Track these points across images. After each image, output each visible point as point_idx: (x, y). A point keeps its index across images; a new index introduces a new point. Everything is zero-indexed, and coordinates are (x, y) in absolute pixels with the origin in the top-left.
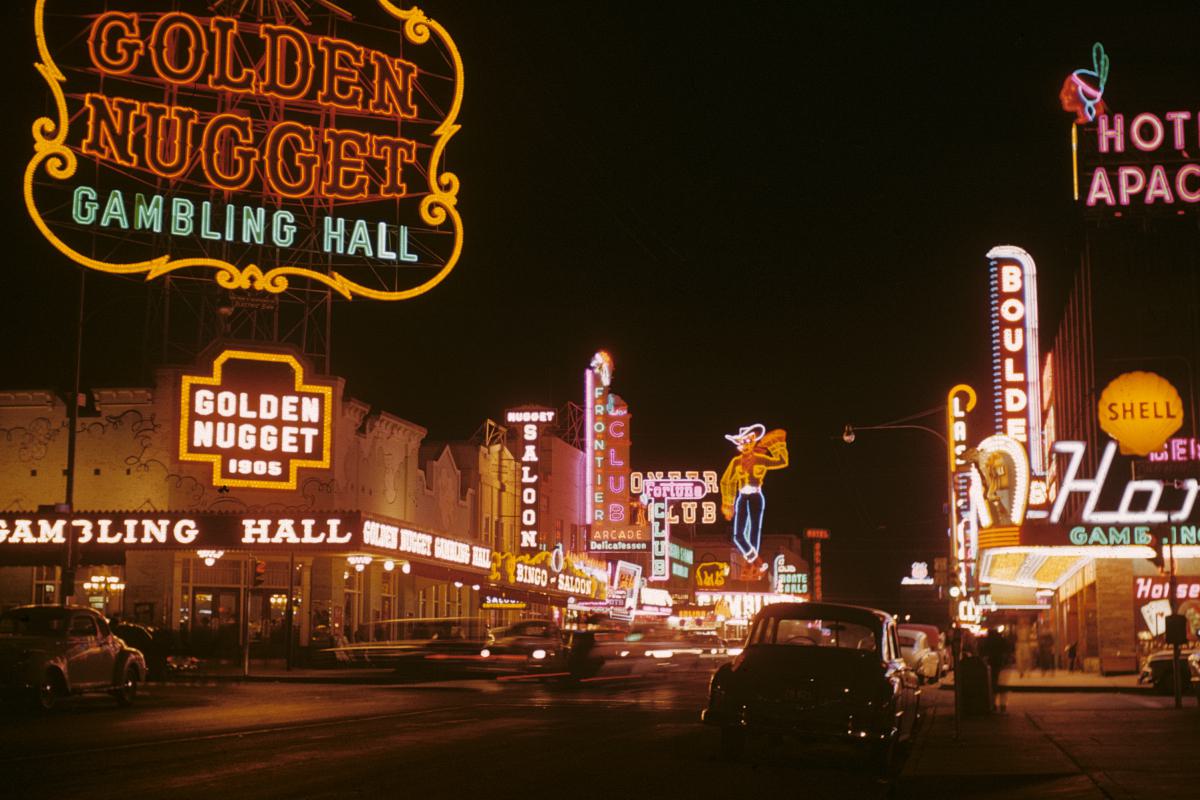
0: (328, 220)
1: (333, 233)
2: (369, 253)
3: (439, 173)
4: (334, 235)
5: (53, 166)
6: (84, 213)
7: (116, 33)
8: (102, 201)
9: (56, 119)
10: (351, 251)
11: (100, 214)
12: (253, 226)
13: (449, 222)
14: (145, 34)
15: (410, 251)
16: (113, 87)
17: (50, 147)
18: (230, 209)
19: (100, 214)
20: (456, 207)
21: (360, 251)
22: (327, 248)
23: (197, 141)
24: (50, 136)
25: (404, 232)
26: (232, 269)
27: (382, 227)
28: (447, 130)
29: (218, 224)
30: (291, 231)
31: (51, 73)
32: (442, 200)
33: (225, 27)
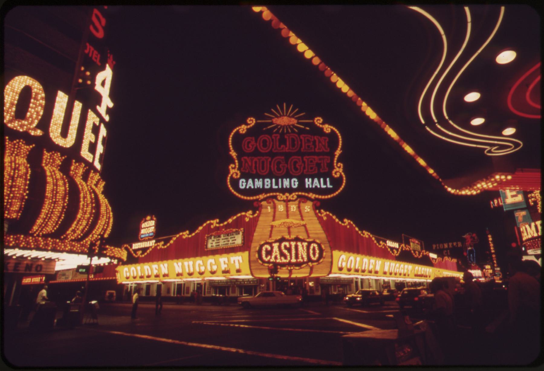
0: (307, 180)
1: (308, 182)
2: (319, 186)
3: (337, 163)
4: (309, 183)
5: (234, 176)
6: (242, 185)
7: (249, 143)
8: (247, 182)
9: (234, 163)
10: (314, 187)
11: (246, 185)
12: (286, 183)
13: (341, 175)
14: (256, 142)
15: (331, 184)
16: (249, 155)
17: (234, 171)
18: (280, 180)
19: (246, 185)
20: (343, 171)
21: (316, 187)
22: (307, 186)
23: (270, 165)
24: (233, 168)
25: (328, 179)
26: (281, 195)
27: (322, 180)
28: (338, 152)
29: (277, 184)
30: (297, 183)
31: (233, 154)
32: (338, 170)
33: (276, 137)
